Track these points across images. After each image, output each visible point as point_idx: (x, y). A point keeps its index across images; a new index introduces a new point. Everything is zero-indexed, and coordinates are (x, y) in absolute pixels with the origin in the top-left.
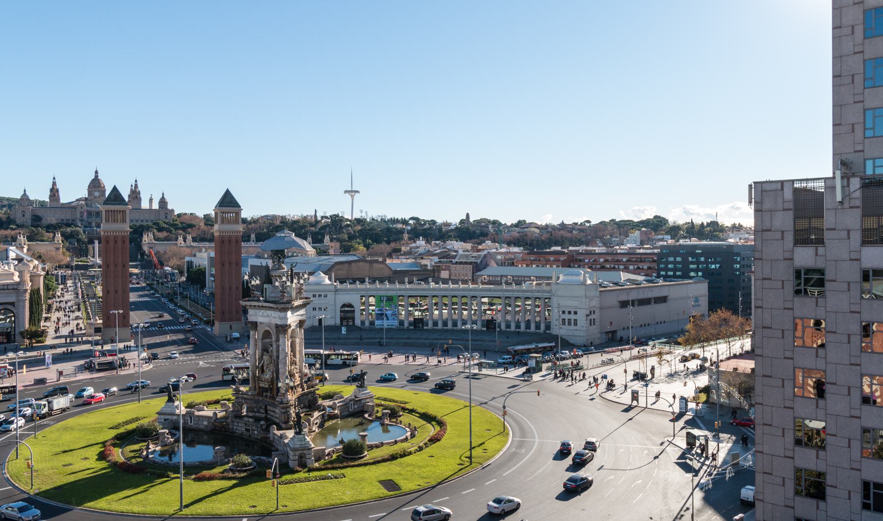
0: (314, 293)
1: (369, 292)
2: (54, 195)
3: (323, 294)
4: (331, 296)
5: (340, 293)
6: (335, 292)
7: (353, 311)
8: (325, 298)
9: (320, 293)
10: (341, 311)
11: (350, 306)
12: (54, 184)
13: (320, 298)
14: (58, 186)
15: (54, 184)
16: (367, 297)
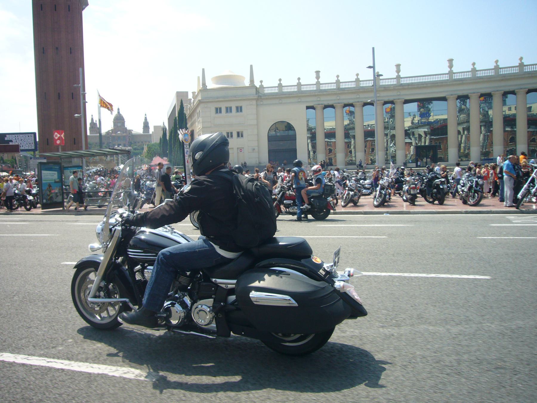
0: (218, 105)
1: (323, 98)
2: (146, 126)
3: (234, 105)
4: (249, 109)
5: (265, 102)
6: (257, 100)
7: (293, 138)
8: (239, 114)
9: (228, 105)
10: (270, 139)
11: (289, 127)
12: (146, 119)
13: (229, 114)
14: (148, 120)
15: (146, 119)
16: (319, 108)
